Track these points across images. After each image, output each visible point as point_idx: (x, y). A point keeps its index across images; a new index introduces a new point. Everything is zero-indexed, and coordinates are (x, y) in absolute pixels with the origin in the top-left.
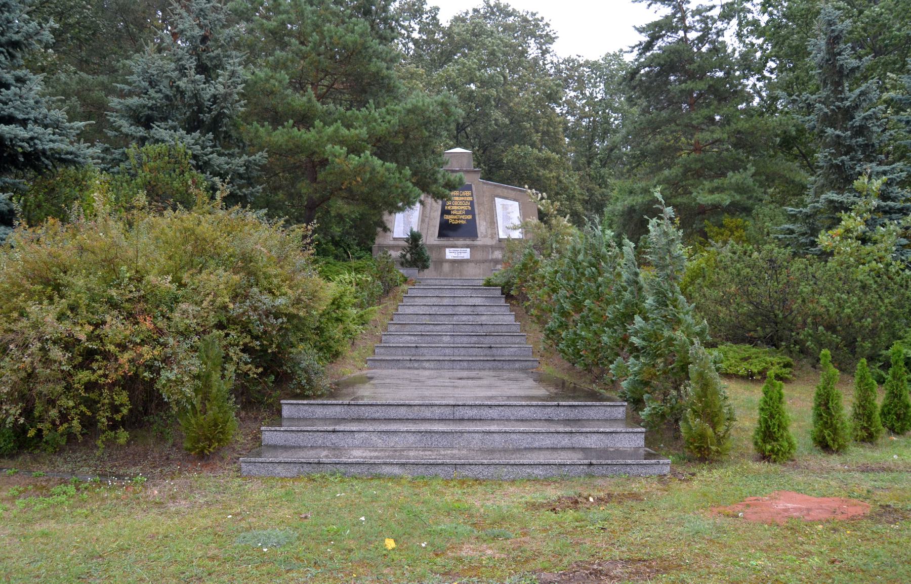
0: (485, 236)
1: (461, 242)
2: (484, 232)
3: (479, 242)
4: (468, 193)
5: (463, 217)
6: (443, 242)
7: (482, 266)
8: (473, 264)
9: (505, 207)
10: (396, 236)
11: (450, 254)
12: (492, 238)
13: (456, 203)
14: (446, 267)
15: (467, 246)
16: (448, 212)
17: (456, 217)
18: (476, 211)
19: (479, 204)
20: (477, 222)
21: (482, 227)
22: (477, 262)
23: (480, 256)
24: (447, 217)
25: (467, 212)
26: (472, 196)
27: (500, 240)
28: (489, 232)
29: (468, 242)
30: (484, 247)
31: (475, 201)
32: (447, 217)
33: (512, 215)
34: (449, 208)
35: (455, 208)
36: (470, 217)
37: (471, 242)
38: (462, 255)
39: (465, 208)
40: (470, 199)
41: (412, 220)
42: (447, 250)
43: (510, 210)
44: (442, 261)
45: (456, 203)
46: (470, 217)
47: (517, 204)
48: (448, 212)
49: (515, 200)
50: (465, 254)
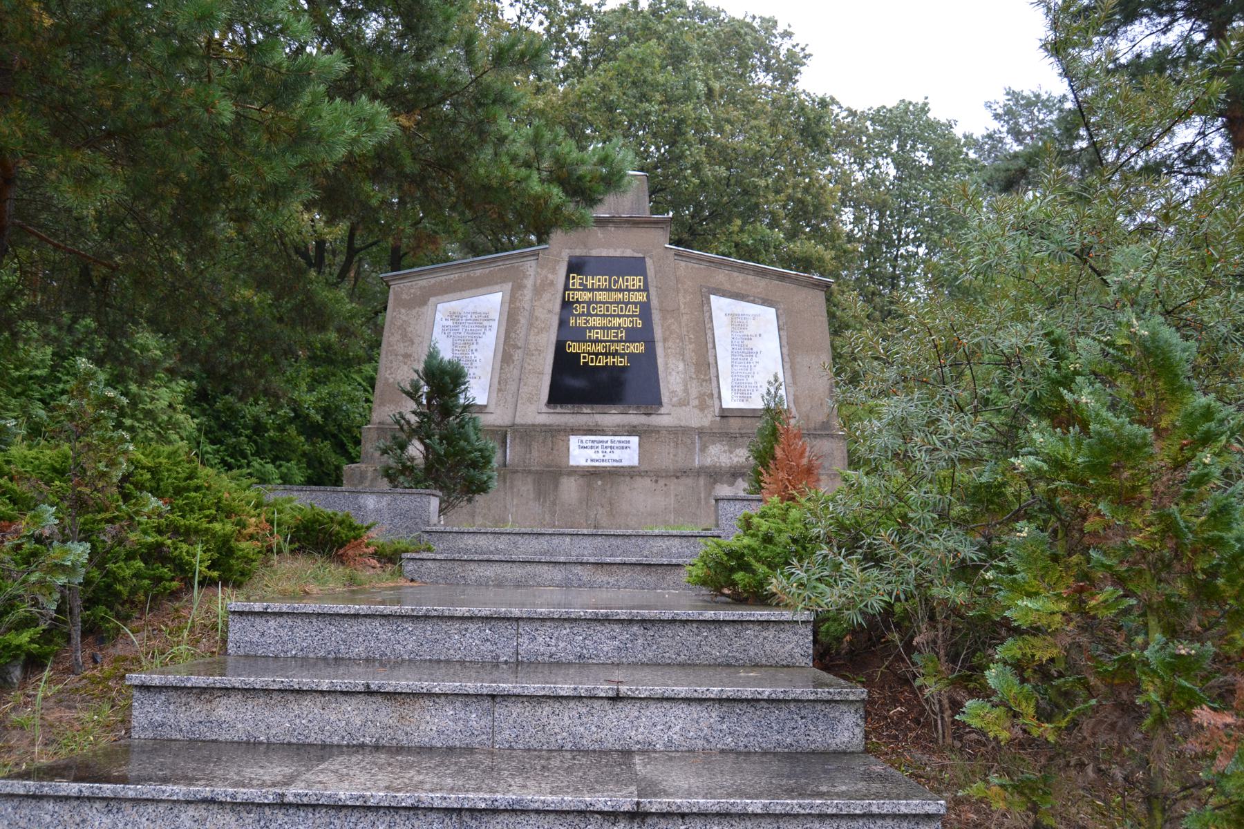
0: (683, 403)
1: (612, 417)
2: (679, 389)
3: (666, 418)
4: (634, 281)
5: (620, 347)
6: (564, 417)
7: (676, 487)
8: (647, 482)
9: (737, 322)
11: (581, 452)
12: (702, 407)
13: (601, 309)
14: (570, 489)
15: (632, 431)
17: (600, 348)
18: (658, 333)
21: (673, 375)
22: (658, 475)
23: (666, 457)
24: (574, 348)
25: (632, 335)
26: (646, 289)
27: (725, 414)
28: (694, 391)
29: (635, 418)
30: (680, 433)
31: (655, 302)
33: (757, 345)
34: (581, 322)
35: (598, 322)
36: (639, 348)
37: (643, 419)
38: (617, 454)
39: (625, 322)
40: (640, 297)
41: (478, 355)
42: (574, 441)
43: (752, 328)
44: (553, 474)
45: (601, 309)
46: (639, 348)
49: (765, 302)
50: (626, 452)
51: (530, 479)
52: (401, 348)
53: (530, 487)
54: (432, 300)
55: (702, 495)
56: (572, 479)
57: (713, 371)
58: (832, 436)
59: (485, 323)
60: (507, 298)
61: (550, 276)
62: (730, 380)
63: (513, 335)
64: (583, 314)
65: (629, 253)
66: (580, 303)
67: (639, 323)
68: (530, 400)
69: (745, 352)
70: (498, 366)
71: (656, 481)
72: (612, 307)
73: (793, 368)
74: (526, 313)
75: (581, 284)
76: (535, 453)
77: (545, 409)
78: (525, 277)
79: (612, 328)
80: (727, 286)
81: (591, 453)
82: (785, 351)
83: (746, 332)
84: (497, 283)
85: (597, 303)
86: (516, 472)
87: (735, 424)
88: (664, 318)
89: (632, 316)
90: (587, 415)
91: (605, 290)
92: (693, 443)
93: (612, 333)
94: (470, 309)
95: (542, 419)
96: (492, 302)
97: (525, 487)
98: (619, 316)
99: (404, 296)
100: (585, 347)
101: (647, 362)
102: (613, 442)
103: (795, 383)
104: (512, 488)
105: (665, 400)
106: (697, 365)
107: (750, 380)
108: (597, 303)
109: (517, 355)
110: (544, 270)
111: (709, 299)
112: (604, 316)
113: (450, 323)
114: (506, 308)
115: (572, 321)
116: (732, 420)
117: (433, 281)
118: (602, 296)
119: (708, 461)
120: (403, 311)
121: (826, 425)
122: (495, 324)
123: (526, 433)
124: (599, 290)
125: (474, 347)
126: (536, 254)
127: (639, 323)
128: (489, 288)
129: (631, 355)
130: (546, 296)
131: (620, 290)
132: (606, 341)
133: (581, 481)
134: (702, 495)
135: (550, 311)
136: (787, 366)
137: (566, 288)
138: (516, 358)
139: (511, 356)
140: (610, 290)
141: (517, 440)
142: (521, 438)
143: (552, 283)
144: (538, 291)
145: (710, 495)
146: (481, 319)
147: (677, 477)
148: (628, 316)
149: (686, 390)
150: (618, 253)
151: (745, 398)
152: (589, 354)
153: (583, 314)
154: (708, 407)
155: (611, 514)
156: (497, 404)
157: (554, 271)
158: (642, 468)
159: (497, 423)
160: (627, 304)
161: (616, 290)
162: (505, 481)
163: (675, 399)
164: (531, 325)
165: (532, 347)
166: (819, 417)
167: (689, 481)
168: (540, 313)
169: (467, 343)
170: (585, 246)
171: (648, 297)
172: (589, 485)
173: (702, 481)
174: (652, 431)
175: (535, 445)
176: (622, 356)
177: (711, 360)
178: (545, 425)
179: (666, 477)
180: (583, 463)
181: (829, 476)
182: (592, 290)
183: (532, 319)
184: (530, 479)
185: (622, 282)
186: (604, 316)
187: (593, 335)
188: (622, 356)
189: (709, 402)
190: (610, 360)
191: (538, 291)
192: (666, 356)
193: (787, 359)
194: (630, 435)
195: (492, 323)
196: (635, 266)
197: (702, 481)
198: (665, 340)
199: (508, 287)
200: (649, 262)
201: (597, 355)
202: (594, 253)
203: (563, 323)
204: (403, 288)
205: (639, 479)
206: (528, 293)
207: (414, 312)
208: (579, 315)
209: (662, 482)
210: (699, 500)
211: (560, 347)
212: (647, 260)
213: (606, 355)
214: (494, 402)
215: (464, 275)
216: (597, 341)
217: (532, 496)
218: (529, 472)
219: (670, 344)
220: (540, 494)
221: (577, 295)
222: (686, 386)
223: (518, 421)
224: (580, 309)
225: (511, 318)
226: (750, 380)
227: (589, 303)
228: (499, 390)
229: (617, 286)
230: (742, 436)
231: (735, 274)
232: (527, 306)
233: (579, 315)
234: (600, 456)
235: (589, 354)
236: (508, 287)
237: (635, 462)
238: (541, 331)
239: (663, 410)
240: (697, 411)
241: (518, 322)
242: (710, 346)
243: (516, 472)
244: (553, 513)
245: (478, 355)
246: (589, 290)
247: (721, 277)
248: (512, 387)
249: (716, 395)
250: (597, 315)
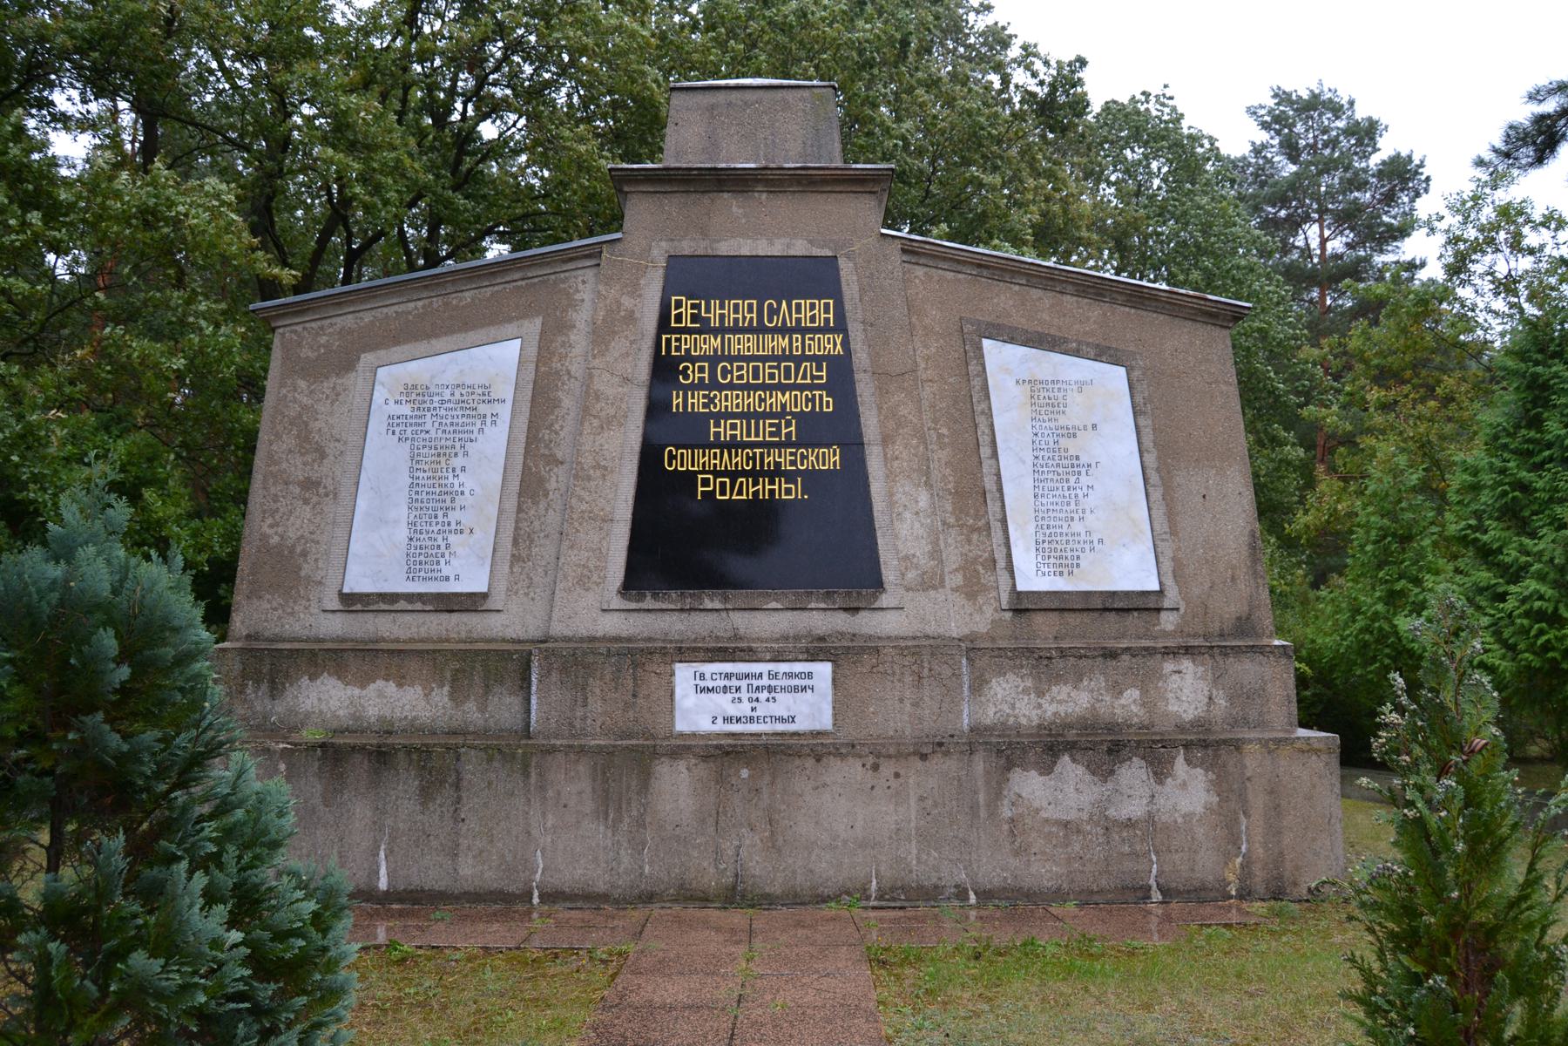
0: (929, 583)
1: (769, 620)
2: (920, 550)
3: (890, 619)
4: (813, 310)
5: (785, 459)
6: (662, 619)
7: (924, 779)
8: (853, 771)
10: (358, 582)
11: (700, 702)
12: (972, 589)
14: (677, 786)
15: (816, 649)
16: (694, 432)
17: (739, 460)
18: (870, 424)
19: (883, 377)
20: (877, 488)
21: (905, 520)
22: (876, 753)
23: (896, 710)
24: (681, 460)
25: (812, 431)
26: (840, 326)
27: (1024, 606)
28: (952, 558)
29: (822, 620)
30: (924, 652)
31: (861, 358)
33: (1088, 447)
34: (697, 401)
36: (828, 459)
37: (840, 622)
38: (784, 704)
40: (829, 345)
41: (467, 481)
42: (684, 675)
43: (1074, 415)
45: (745, 373)
46: (828, 459)
47: (1115, 377)
49: (1104, 353)
50: (806, 701)
51: (583, 768)
52: (297, 468)
53: (585, 785)
54: (367, 358)
55: (981, 798)
56: (682, 765)
57: (993, 507)
58: (1260, 650)
59: (483, 409)
60: (533, 351)
61: (627, 302)
62: (1031, 528)
63: (545, 434)
64: (701, 385)
65: (800, 248)
66: (693, 360)
67: (828, 404)
68: (583, 582)
69: (1062, 466)
70: (511, 504)
71: (875, 767)
72: (766, 369)
73: (1168, 499)
74: (575, 386)
75: (694, 318)
76: (596, 705)
77: (618, 603)
78: (573, 305)
79: (766, 415)
80: (1018, 320)
81: (724, 703)
82: (1151, 459)
83: (1063, 421)
84: (510, 320)
85: (731, 359)
86: (552, 750)
87: (1045, 628)
88: (882, 391)
89: (811, 387)
90: (711, 617)
91: (750, 330)
92: (957, 676)
93: (767, 426)
94: (450, 377)
95: (612, 625)
96: (498, 360)
97: (574, 785)
98: (783, 388)
99: (306, 352)
100: (706, 459)
101: (845, 504)
102: (773, 675)
103: (1173, 532)
104: (542, 788)
105: (889, 575)
106: (958, 494)
107: (1077, 527)
108: (731, 359)
109: (557, 480)
110: (617, 298)
111: (980, 348)
112: (747, 387)
113: (406, 409)
114: (530, 375)
115: (677, 401)
116: (1039, 618)
117: (367, 317)
118: (744, 344)
119: (989, 715)
120: (302, 384)
121: (1244, 626)
122: (505, 411)
123: (576, 659)
124: (736, 330)
125: (457, 462)
126: (594, 253)
127: (828, 404)
128: (493, 331)
129: (811, 477)
130: (618, 346)
131: (783, 330)
132: (752, 445)
133: (703, 770)
134: (981, 798)
135: (626, 380)
136: (1157, 495)
137: (663, 325)
138: (552, 485)
139: (541, 481)
140: (761, 330)
141: (555, 676)
142: (564, 670)
143: (631, 318)
144: (601, 336)
145: (998, 795)
146: (473, 400)
147: (924, 757)
148: (801, 388)
149: (936, 554)
150: (777, 249)
151: (1067, 566)
152: (717, 474)
153: (701, 385)
154: (985, 589)
155: (773, 846)
156: (511, 591)
157: (635, 290)
158: (842, 737)
159: (511, 633)
160: (798, 360)
161: (775, 330)
162: (526, 774)
163: (911, 575)
164: (585, 411)
165: (588, 461)
166: (1229, 608)
167: (951, 765)
168: (605, 385)
169: (443, 453)
170: (705, 235)
171: (846, 343)
172: (721, 779)
173: (979, 764)
174: (863, 650)
175: (595, 686)
176: (790, 477)
177: (989, 483)
178: (617, 639)
179: (899, 756)
180: (705, 725)
181: (1264, 743)
182: (721, 331)
183: (589, 395)
184: (583, 768)
186: (747, 387)
187: (724, 431)
188: (790, 477)
189: (987, 578)
190: (764, 488)
191: (601, 336)
192: (890, 476)
193: (1154, 478)
194: (813, 657)
195: (497, 408)
196: (815, 276)
197: (979, 764)
198: (886, 440)
199: (534, 326)
200: (845, 267)
201: (734, 475)
202: (725, 248)
203: (656, 409)
204: (298, 339)
205: (835, 763)
206: (579, 340)
207: (327, 386)
208: (693, 387)
209: (887, 769)
210: (974, 808)
211: (650, 457)
212: (842, 262)
213: (755, 475)
214: (502, 586)
215: (437, 303)
216: (733, 445)
217: (589, 806)
218: (582, 750)
219: (898, 448)
220: (608, 803)
221: (688, 342)
222: (936, 543)
223: (557, 629)
225: (541, 393)
226: (1077, 527)
227: (714, 360)
228: (515, 559)
229: (777, 322)
230: (1063, 654)
231: (1036, 293)
232: (576, 369)
233: (693, 387)
234: (744, 709)
235: (717, 474)
236: (534, 326)
237: (825, 721)
238: (607, 423)
239: (885, 600)
240: (960, 599)
241: (556, 404)
242: (985, 451)
243: (552, 750)
244: (638, 846)
245: (467, 481)
246: (715, 332)
247: (1004, 300)
248: (544, 551)
249: (1001, 563)
250: (731, 386)
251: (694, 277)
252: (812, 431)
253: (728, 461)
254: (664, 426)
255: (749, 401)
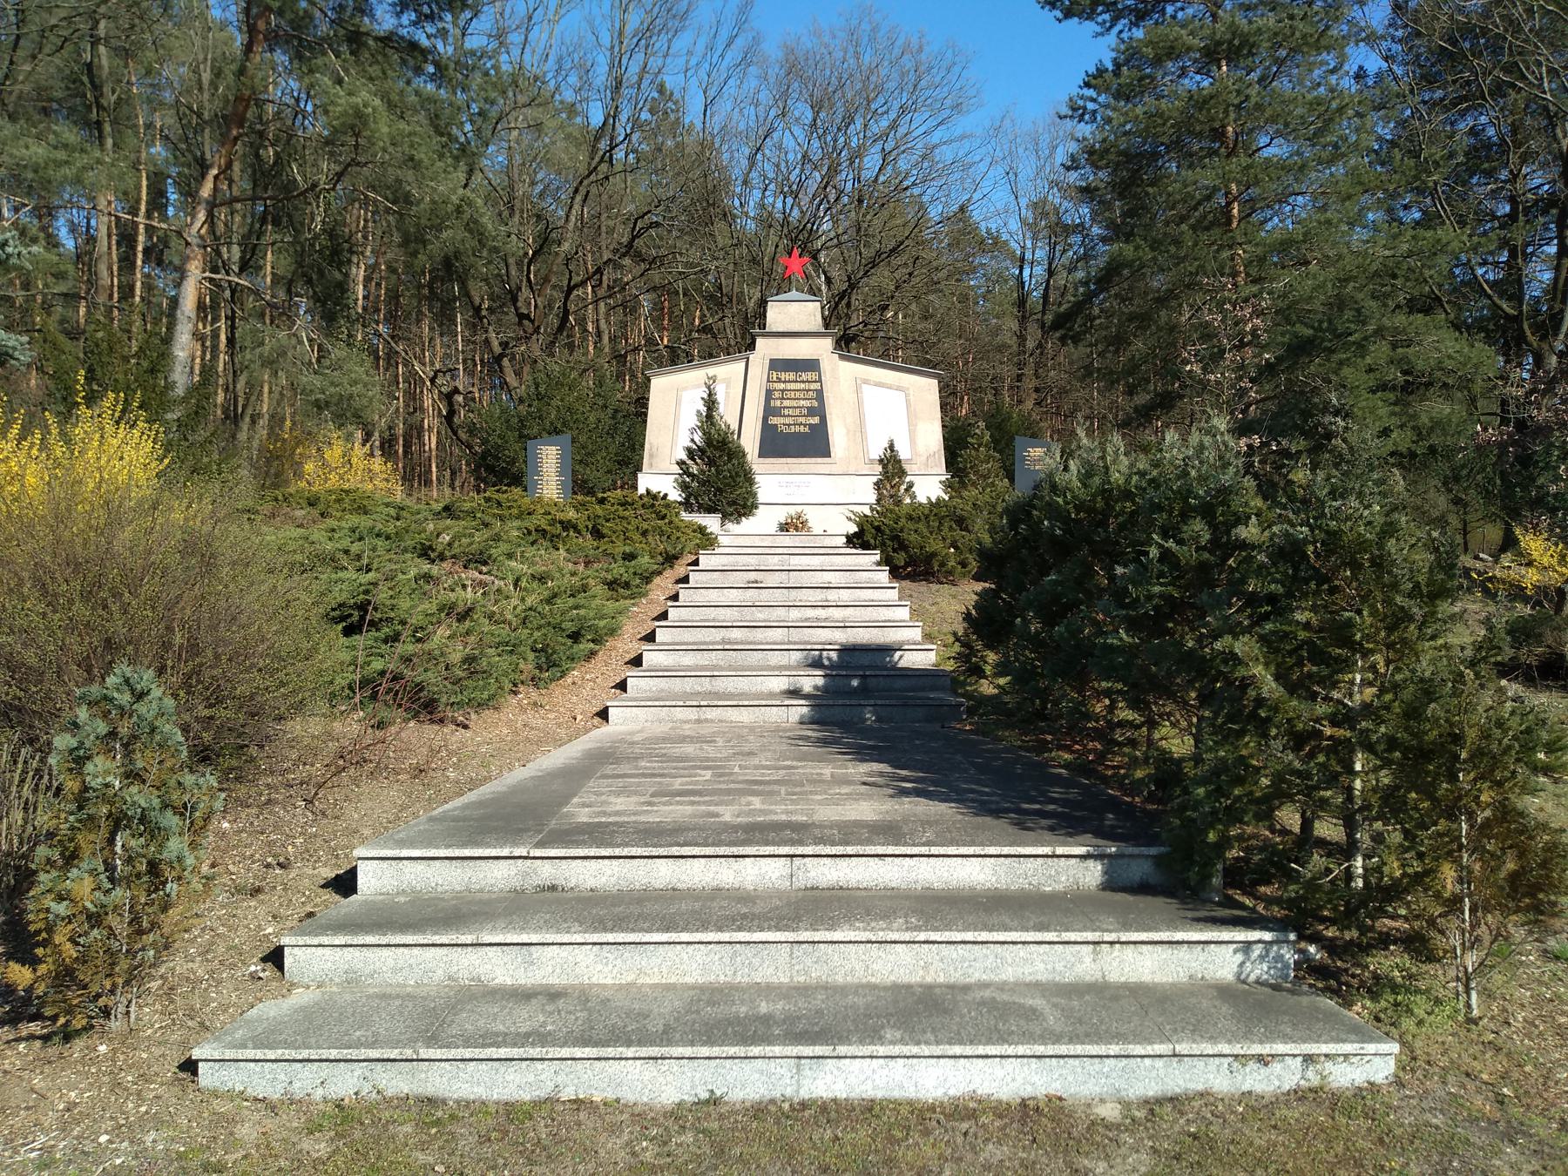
16: (777, 412)
24: (774, 420)
25: (811, 412)
26: (820, 381)
32: (774, 420)
34: (778, 403)
35: (786, 403)
36: (815, 420)
39: (807, 403)
48: (777, 412)
49: (899, 389)
67: (816, 404)
127: (816, 404)
185: (804, 377)
196: (812, 365)
211: (765, 419)
224: (777, 394)
251: (777, 365)
252: (811, 412)
253: (787, 421)
254: (769, 411)
255: (794, 403)
